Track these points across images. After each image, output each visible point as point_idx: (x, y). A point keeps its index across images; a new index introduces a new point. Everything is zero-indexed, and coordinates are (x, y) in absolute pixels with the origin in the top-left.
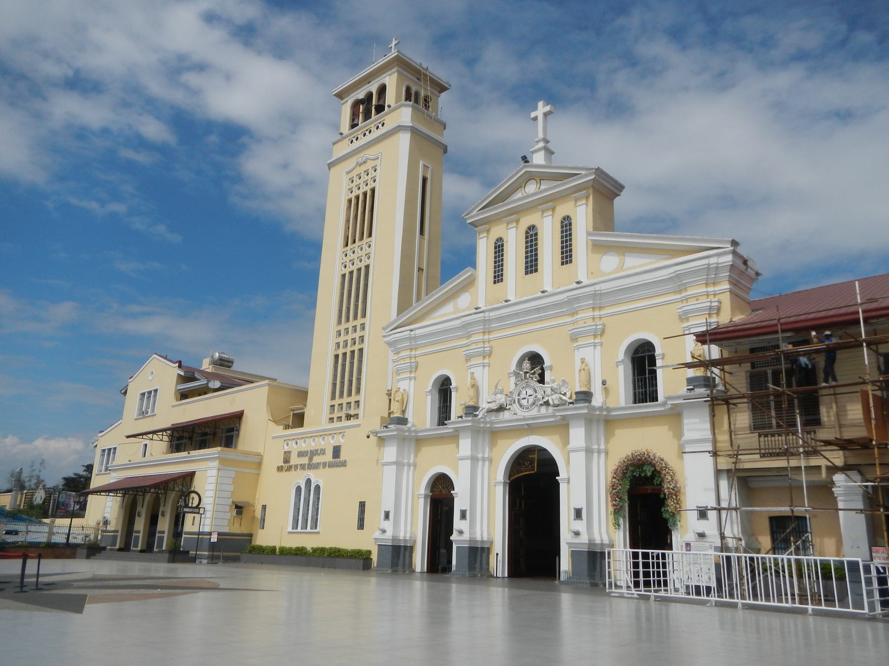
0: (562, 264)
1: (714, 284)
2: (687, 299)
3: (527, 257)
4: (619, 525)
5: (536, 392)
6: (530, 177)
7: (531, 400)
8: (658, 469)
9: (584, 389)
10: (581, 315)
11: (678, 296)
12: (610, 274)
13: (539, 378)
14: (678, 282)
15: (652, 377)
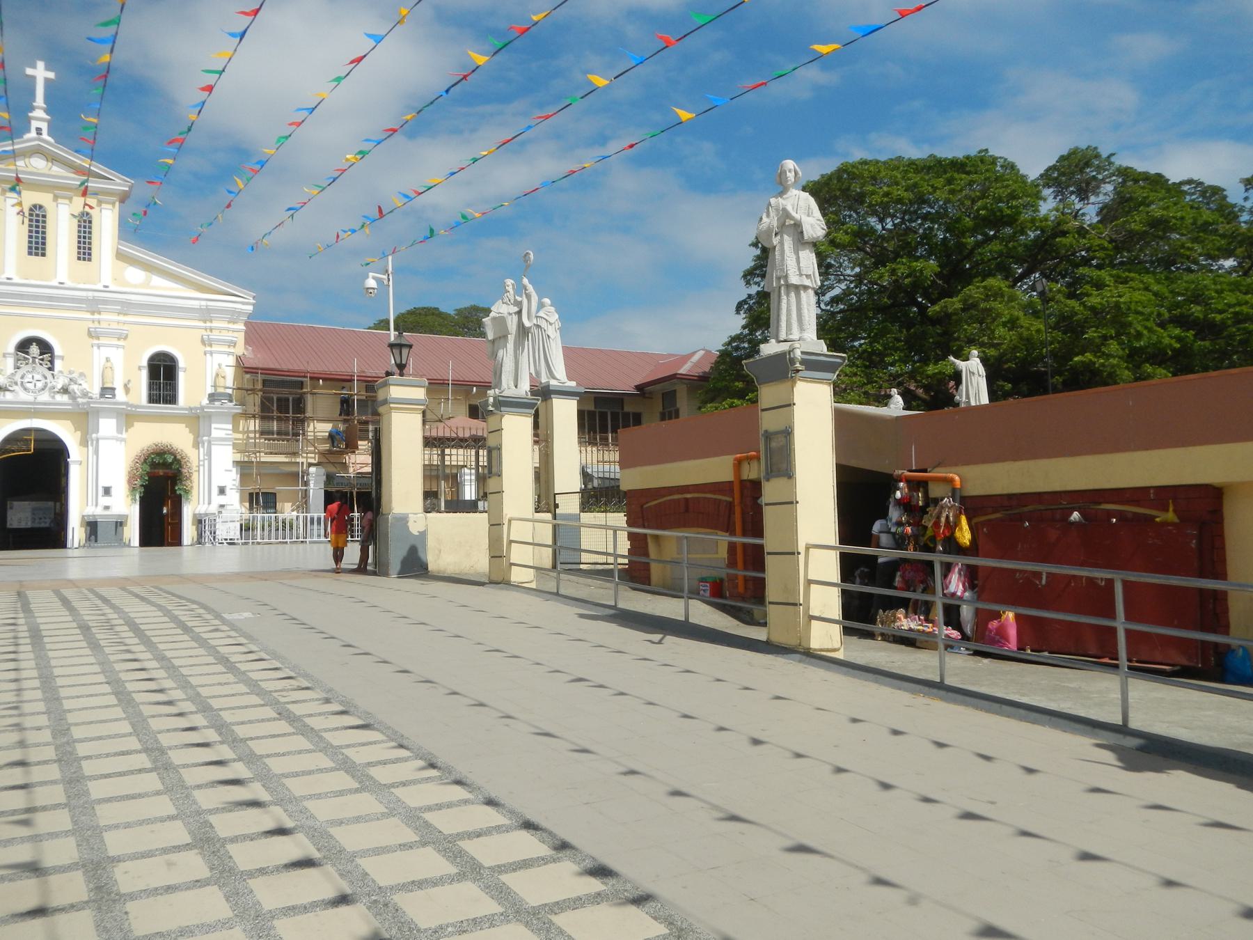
0: (79, 259)
1: (234, 323)
2: (211, 330)
3: (30, 237)
4: (135, 500)
5: (46, 378)
6: (38, 151)
7: (40, 385)
8: (179, 457)
9: (107, 385)
10: (104, 316)
11: (201, 324)
12: (135, 286)
13: (49, 365)
14: (206, 314)
15: (167, 384)
